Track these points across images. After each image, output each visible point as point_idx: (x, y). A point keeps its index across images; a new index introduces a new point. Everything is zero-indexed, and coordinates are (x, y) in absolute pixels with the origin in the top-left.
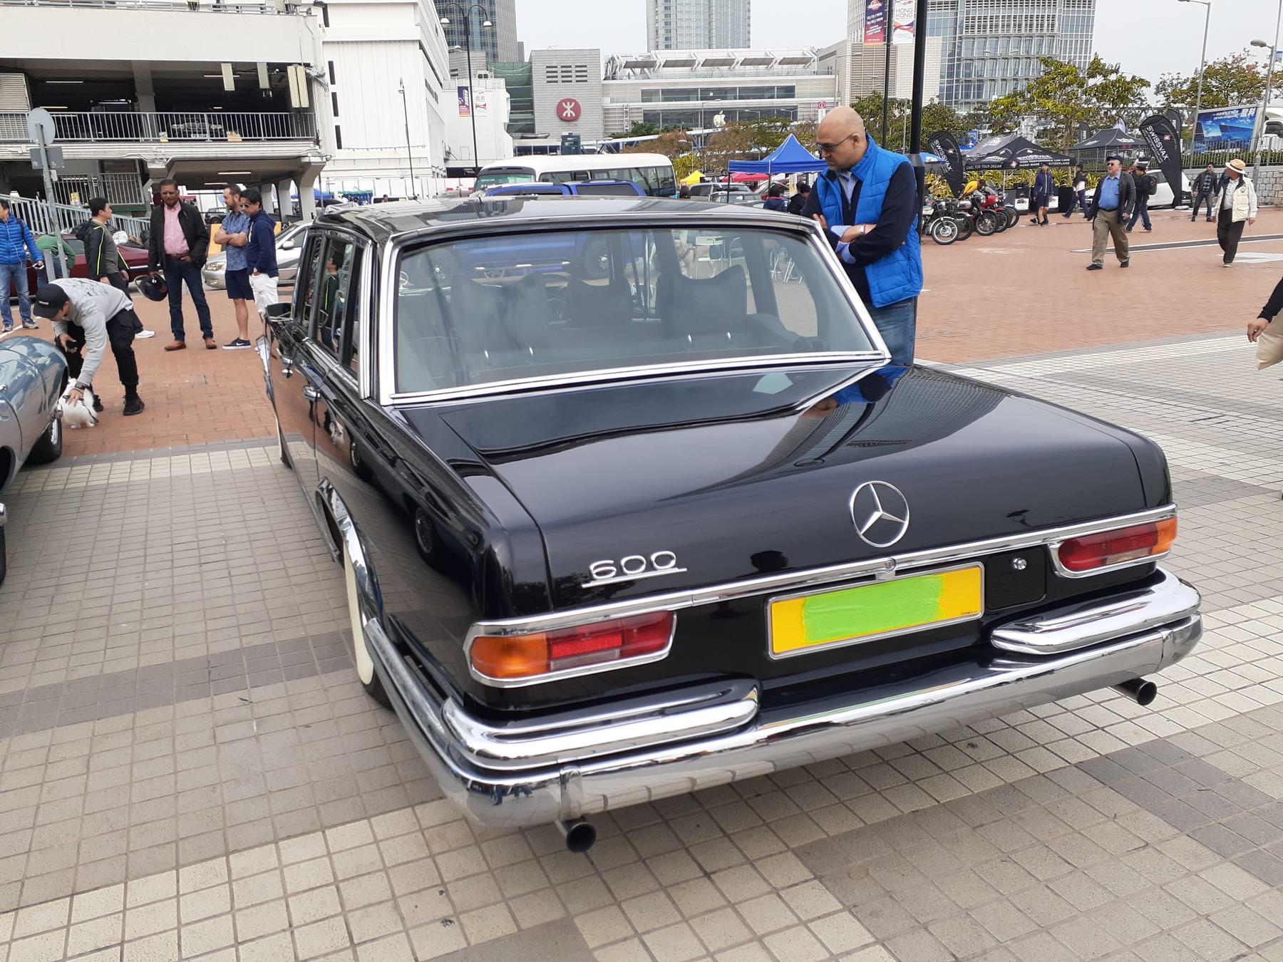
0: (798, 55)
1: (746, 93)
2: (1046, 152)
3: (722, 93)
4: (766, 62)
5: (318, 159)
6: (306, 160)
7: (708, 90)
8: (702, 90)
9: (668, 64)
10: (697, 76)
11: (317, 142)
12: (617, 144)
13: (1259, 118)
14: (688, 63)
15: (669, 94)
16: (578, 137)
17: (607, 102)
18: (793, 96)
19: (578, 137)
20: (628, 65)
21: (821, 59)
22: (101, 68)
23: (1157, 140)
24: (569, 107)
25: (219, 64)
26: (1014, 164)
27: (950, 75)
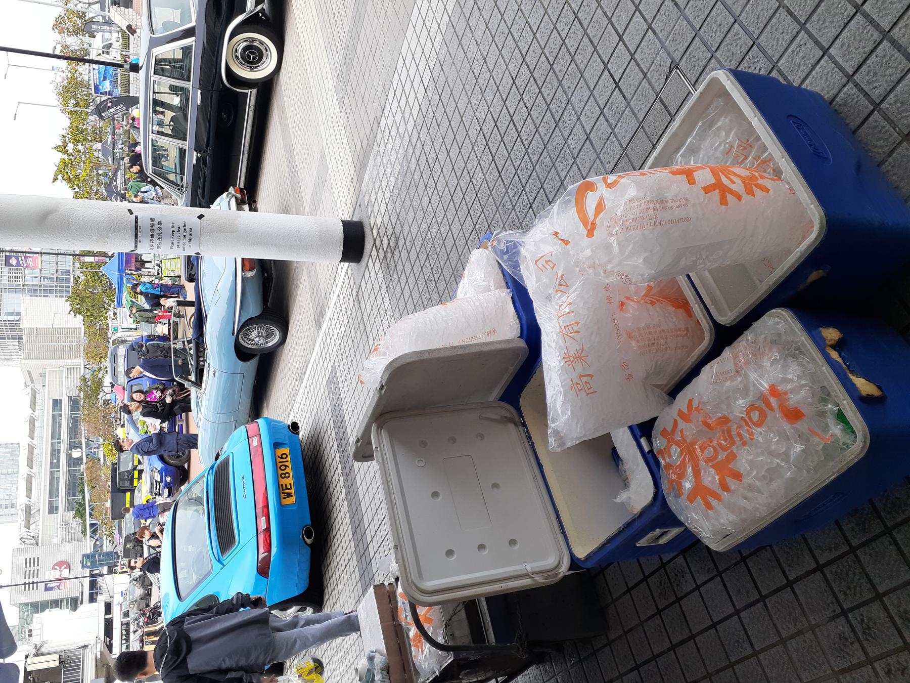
0: (28, 398)
1: (55, 434)
2: (115, 175)
3: (55, 453)
4: (32, 421)
7: (51, 463)
8: (51, 467)
9: (29, 494)
10: (40, 473)
11: (85, 647)
12: (92, 525)
14: (29, 479)
15: (53, 491)
16: (84, 556)
18: (61, 400)
19: (84, 556)
20: (28, 526)
21: (33, 382)
23: (110, 111)
27: (51, 291)
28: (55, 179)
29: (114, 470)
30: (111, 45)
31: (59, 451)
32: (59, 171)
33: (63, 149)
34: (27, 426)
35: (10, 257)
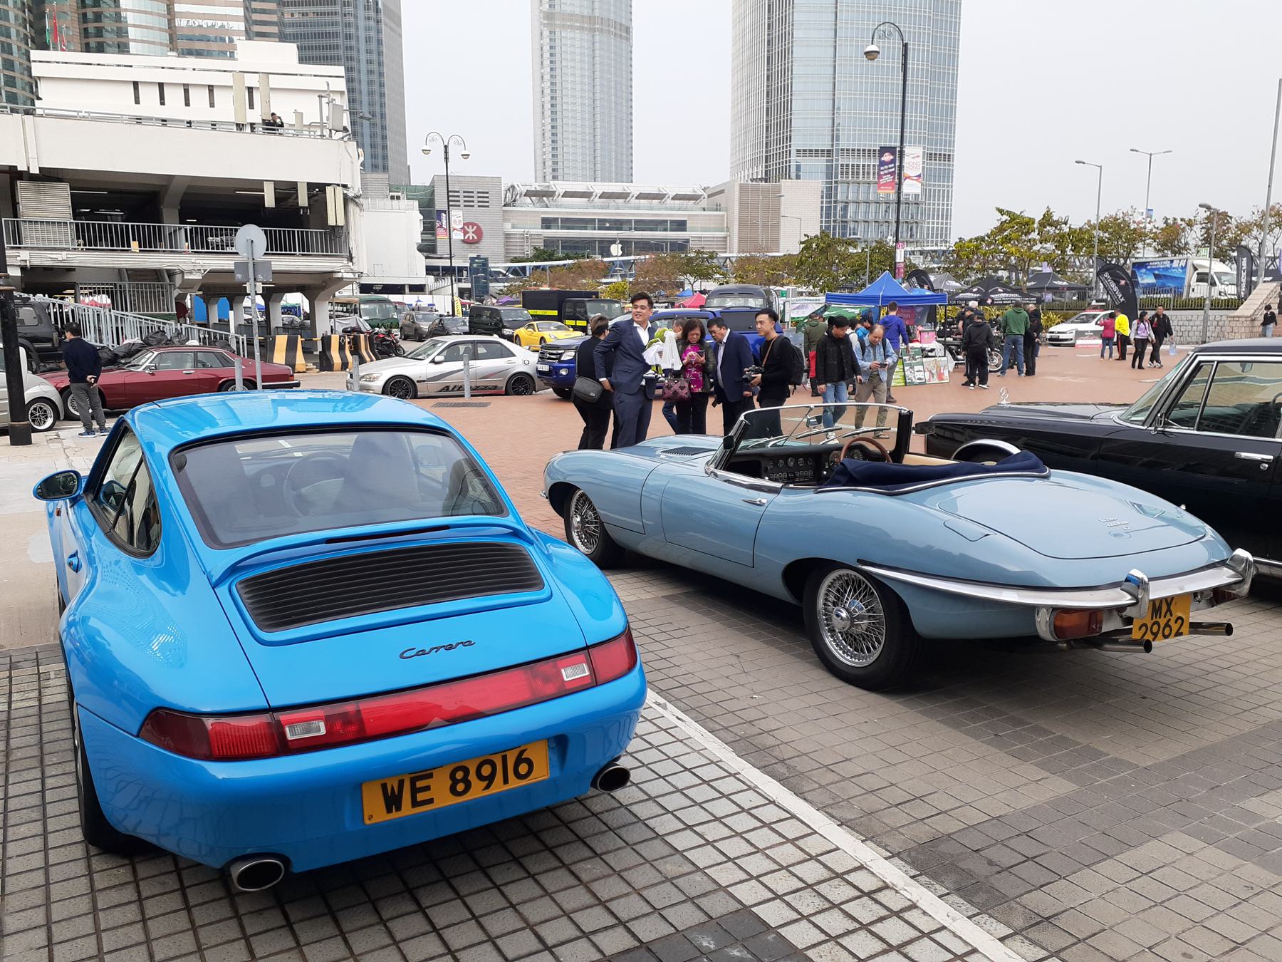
1: (642, 225)
3: (618, 224)
4: (659, 197)
5: (351, 276)
6: (339, 275)
9: (567, 194)
11: (350, 259)
12: (524, 269)
13: (1190, 268)
14: (586, 195)
15: (568, 223)
16: (486, 259)
17: (508, 227)
19: (486, 259)
22: (134, 180)
23: (1113, 285)
24: (471, 230)
25: (262, 182)
26: (989, 301)
27: (828, 216)
28: (1001, 211)
29: (588, 295)
30: (1213, 284)
31: (621, 229)
32: (1013, 217)
33: (1047, 220)
34: (653, 190)
35: (893, 153)
